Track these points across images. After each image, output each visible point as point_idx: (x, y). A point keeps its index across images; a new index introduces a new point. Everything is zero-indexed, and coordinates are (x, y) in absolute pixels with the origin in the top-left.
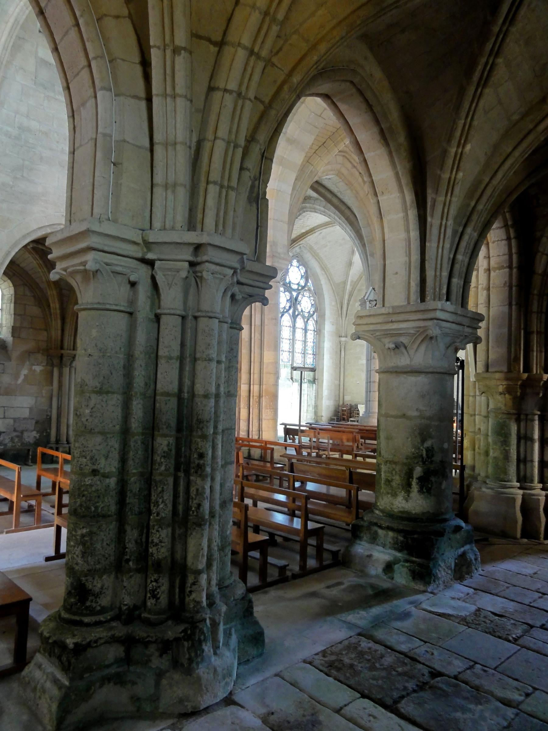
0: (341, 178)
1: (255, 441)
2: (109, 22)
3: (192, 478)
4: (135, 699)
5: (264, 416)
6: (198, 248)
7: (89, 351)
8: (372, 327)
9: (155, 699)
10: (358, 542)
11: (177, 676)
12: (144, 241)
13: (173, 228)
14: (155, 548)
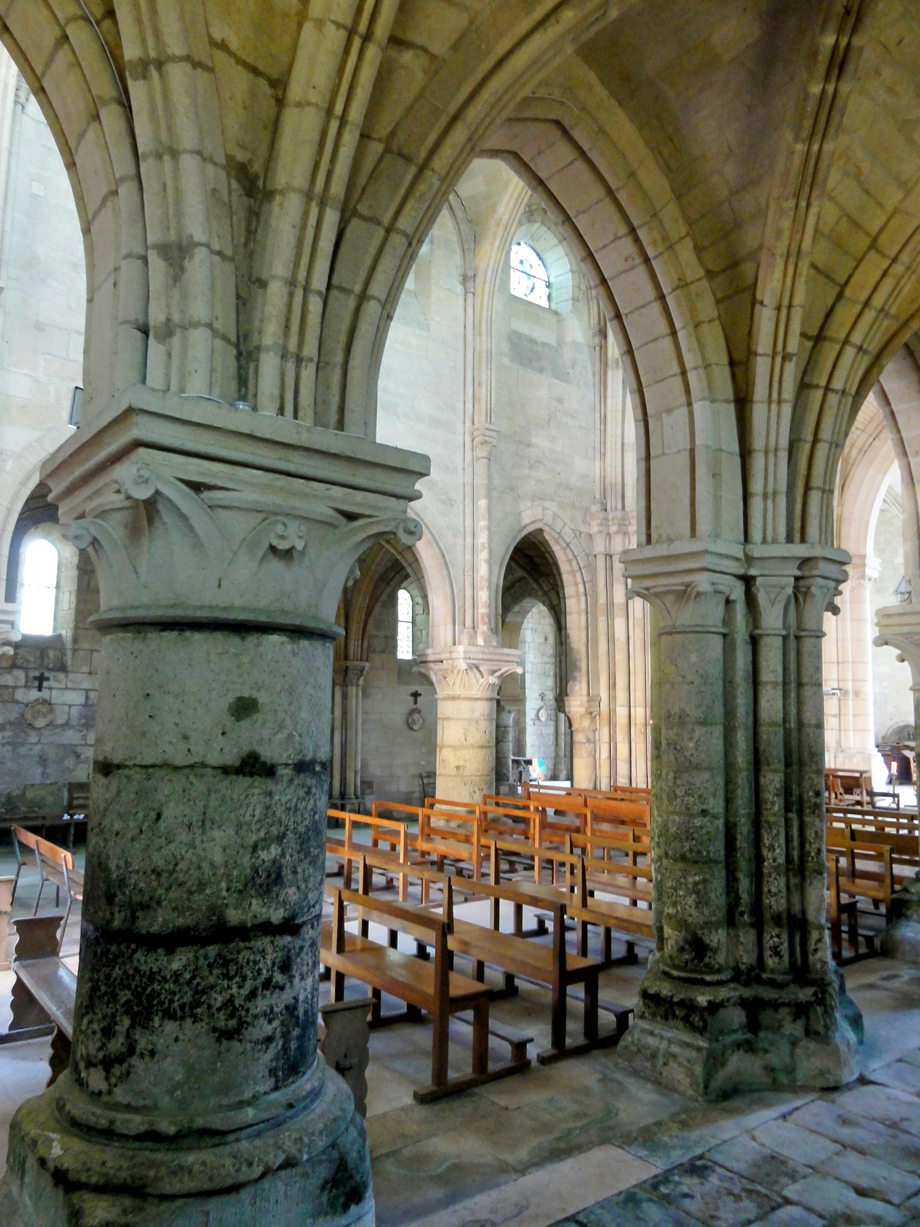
1: (624, 790)
2: (705, 327)
3: (807, 819)
4: (770, 1069)
6: (805, 562)
7: (690, 678)
8: (906, 629)
9: (790, 1071)
10: (904, 922)
11: (812, 1045)
12: (746, 555)
13: (774, 541)
14: (773, 900)
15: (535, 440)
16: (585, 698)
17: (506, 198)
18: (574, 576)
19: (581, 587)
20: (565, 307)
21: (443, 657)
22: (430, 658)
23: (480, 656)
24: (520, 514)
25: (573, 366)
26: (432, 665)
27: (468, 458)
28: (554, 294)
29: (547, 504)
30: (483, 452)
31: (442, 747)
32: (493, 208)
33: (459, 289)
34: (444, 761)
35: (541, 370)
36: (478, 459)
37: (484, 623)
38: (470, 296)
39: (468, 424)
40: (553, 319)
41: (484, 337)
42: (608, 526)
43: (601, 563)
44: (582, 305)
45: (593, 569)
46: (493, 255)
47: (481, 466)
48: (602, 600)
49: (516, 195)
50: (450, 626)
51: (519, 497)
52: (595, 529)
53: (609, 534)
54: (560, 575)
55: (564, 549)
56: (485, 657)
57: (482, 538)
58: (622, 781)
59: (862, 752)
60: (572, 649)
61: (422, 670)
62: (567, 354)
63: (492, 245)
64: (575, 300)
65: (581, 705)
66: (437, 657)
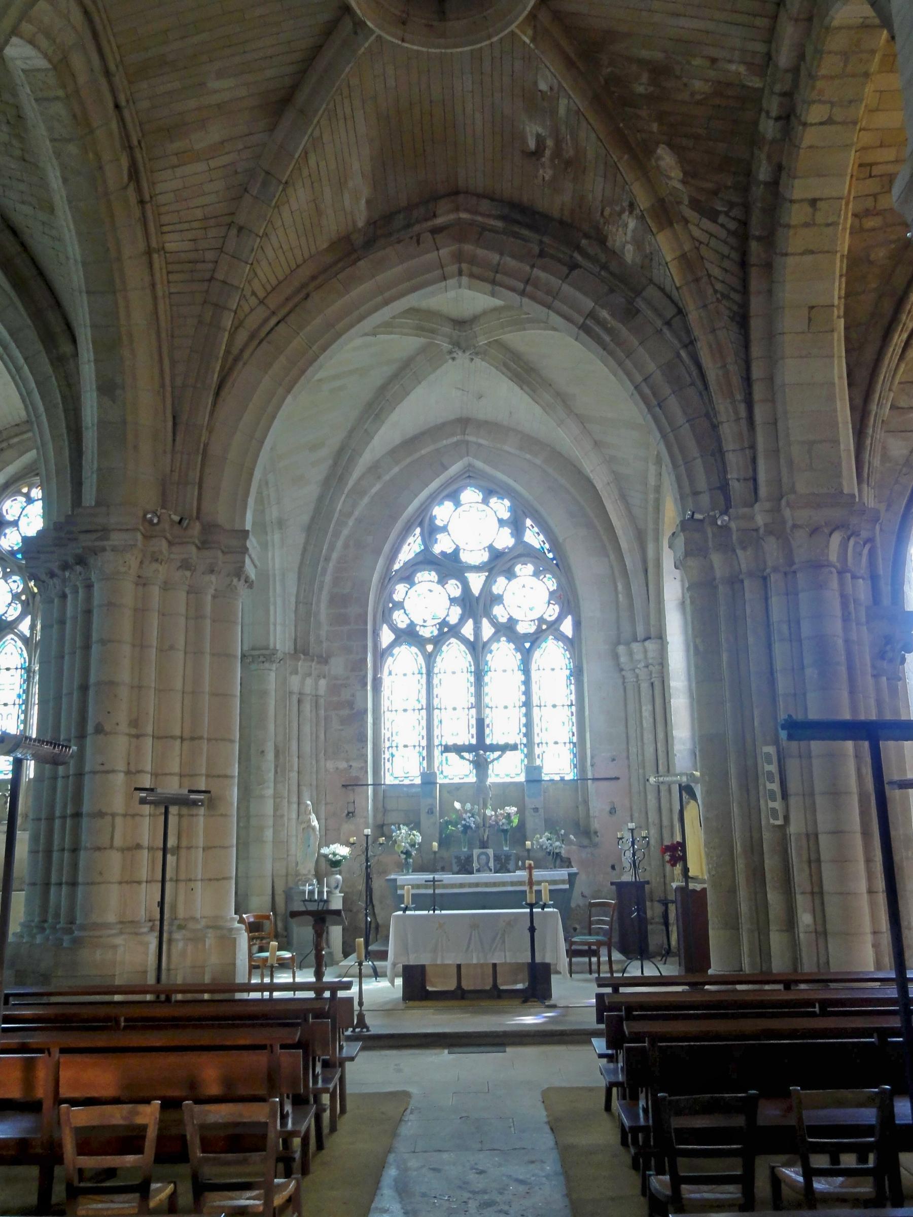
0: (64, 86)
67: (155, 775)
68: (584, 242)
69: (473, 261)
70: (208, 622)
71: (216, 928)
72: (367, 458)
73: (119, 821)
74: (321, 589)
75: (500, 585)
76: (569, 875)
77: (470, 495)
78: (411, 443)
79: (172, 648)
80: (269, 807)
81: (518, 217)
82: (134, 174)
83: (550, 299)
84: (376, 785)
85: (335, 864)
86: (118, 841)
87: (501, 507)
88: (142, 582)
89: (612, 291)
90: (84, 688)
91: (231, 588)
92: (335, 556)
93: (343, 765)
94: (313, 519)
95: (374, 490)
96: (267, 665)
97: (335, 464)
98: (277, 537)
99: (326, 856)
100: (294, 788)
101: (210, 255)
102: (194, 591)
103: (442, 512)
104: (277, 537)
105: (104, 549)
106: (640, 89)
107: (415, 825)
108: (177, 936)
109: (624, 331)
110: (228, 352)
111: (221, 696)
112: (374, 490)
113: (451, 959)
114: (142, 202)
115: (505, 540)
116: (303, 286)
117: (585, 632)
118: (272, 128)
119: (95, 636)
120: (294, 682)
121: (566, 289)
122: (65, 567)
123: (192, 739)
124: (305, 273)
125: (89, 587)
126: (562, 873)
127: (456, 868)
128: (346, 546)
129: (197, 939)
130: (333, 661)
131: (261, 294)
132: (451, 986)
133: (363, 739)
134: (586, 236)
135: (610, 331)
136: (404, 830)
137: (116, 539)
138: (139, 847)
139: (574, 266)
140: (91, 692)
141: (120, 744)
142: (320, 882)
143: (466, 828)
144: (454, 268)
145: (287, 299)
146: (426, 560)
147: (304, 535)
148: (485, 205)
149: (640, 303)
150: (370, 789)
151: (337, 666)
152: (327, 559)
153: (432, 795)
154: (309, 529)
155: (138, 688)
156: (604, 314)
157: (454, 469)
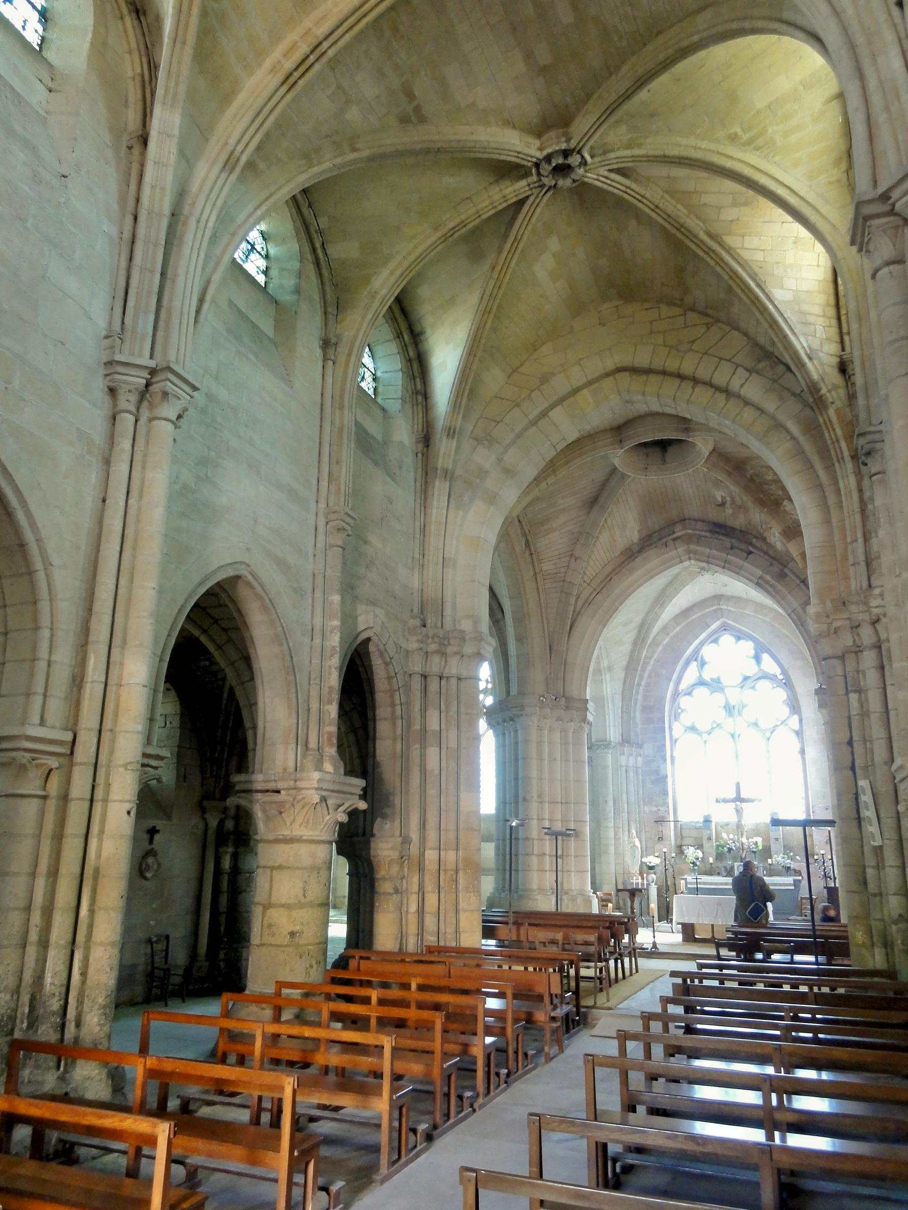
5: (462, 905)
15: (372, 538)
16: (400, 839)
17: (385, 273)
18: (392, 696)
19: (398, 708)
20: (394, 406)
21: (280, 785)
22: (258, 786)
23: (331, 787)
24: (356, 618)
25: (400, 467)
26: (259, 796)
27: (321, 544)
28: (380, 389)
29: (378, 611)
30: (339, 539)
31: (267, 907)
32: (367, 279)
33: (319, 352)
34: (270, 925)
35: (377, 464)
36: (332, 546)
37: (330, 744)
38: (330, 363)
39: (322, 505)
40: (380, 414)
41: (346, 412)
42: (427, 644)
43: (416, 683)
44: (408, 406)
45: (408, 688)
46: (364, 327)
47: (335, 555)
48: (417, 727)
49: (398, 273)
50: (294, 746)
51: (356, 597)
52: (413, 645)
53: (427, 652)
54: (372, 692)
55: (387, 664)
56: (336, 788)
57: (335, 640)
58: (431, 940)
59: (582, 893)
60: (381, 780)
61: (243, 802)
62: (393, 454)
63: (363, 318)
64: (403, 400)
65: (393, 848)
66: (271, 786)
67: (550, 820)
68: (754, 540)
69: (695, 553)
70: (571, 746)
71: (582, 895)
72: (659, 624)
73: (535, 842)
74: (636, 703)
75: (747, 695)
76: (794, 881)
77: (727, 639)
78: (686, 612)
79: (555, 759)
80: (611, 834)
81: (718, 530)
82: (527, 544)
83: (738, 570)
84: (676, 821)
85: (651, 868)
86: (536, 852)
87: (748, 647)
88: (540, 729)
89: (771, 564)
90: (516, 779)
91: (581, 728)
92: (643, 683)
93: (655, 809)
94: (629, 662)
95: (665, 642)
96: (606, 750)
97: (639, 631)
98: (608, 676)
99: (645, 863)
100: (626, 823)
101: (563, 570)
102: (564, 731)
103: (708, 651)
104: (608, 676)
105: (522, 715)
106: (770, 478)
107: (700, 847)
108: (564, 897)
109: (779, 587)
110: (574, 611)
111: (579, 781)
112: (665, 642)
113: (707, 921)
114: (531, 554)
115: (752, 669)
116: (608, 575)
117: (805, 727)
118: (588, 513)
119: (520, 756)
120: (623, 760)
121: (746, 564)
122: (504, 721)
123: (567, 803)
124: (609, 569)
125: (516, 731)
126: (790, 880)
127: (724, 874)
128: (650, 676)
129: (573, 899)
130: (645, 746)
131: (588, 581)
132: (709, 936)
133: (665, 793)
134: (756, 537)
135: (772, 586)
136: (692, 849)
137: (528, 710)
138: (544, 854)
139: (750, 553)
140: (520, 782)
141: (534, 806)
142: (643, 879)
143: (730, 850)
144: (687, 556)
145: (601, 582)
146: (701, 683)
147: (624, 673)
148: (700, 525)
149: (786, 571)
150: (672, 824)
151: (648, 749)
152: (639, 685)
153: (709, 829)
154: (627, 668)
155: (540, 779)
156: (768, 577)
157: (714, 627)
